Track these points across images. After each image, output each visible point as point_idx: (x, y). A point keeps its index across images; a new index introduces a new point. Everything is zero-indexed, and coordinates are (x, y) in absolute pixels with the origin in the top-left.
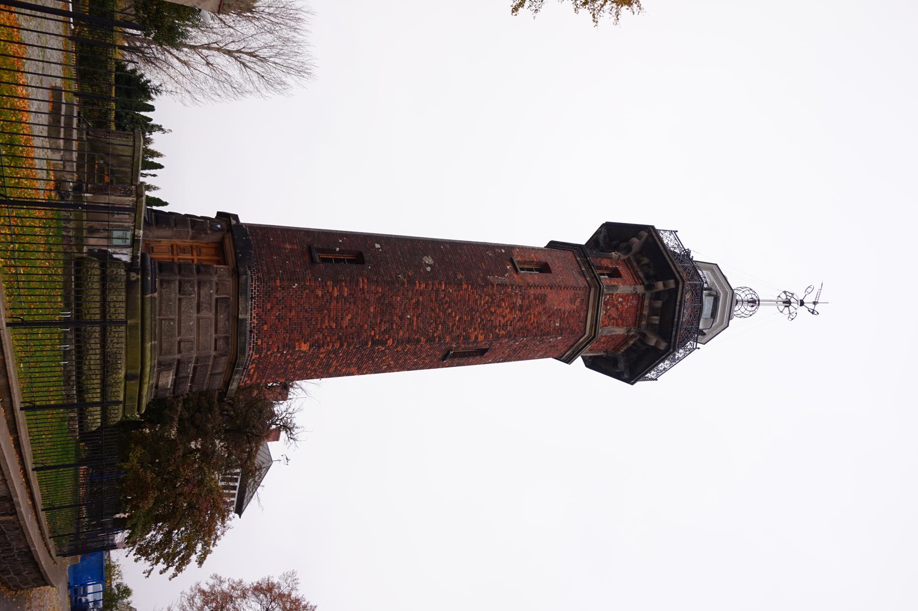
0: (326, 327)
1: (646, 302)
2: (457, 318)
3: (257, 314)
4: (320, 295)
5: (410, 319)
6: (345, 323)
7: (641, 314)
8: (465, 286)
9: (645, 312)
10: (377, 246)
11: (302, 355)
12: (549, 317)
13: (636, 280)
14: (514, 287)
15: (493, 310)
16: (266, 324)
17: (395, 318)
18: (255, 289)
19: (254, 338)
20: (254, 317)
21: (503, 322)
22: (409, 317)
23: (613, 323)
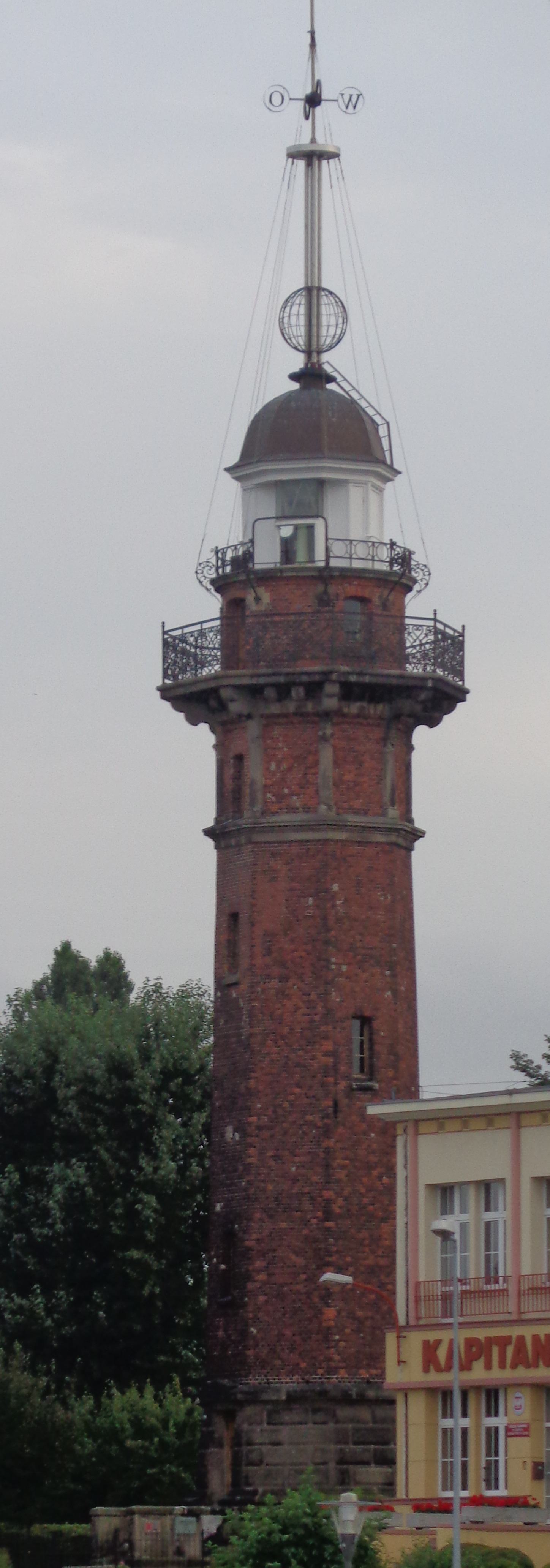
1: (275, 709)
2: (297, 1090)
5: (298, 1167)
11: (344, 1314)
14: (253, 996)
16: (298, 1364)
17: (295, 1191)
19: (315, 1378)
20: (291, 1379)
22: (294, 1169)
23: (314, 774)
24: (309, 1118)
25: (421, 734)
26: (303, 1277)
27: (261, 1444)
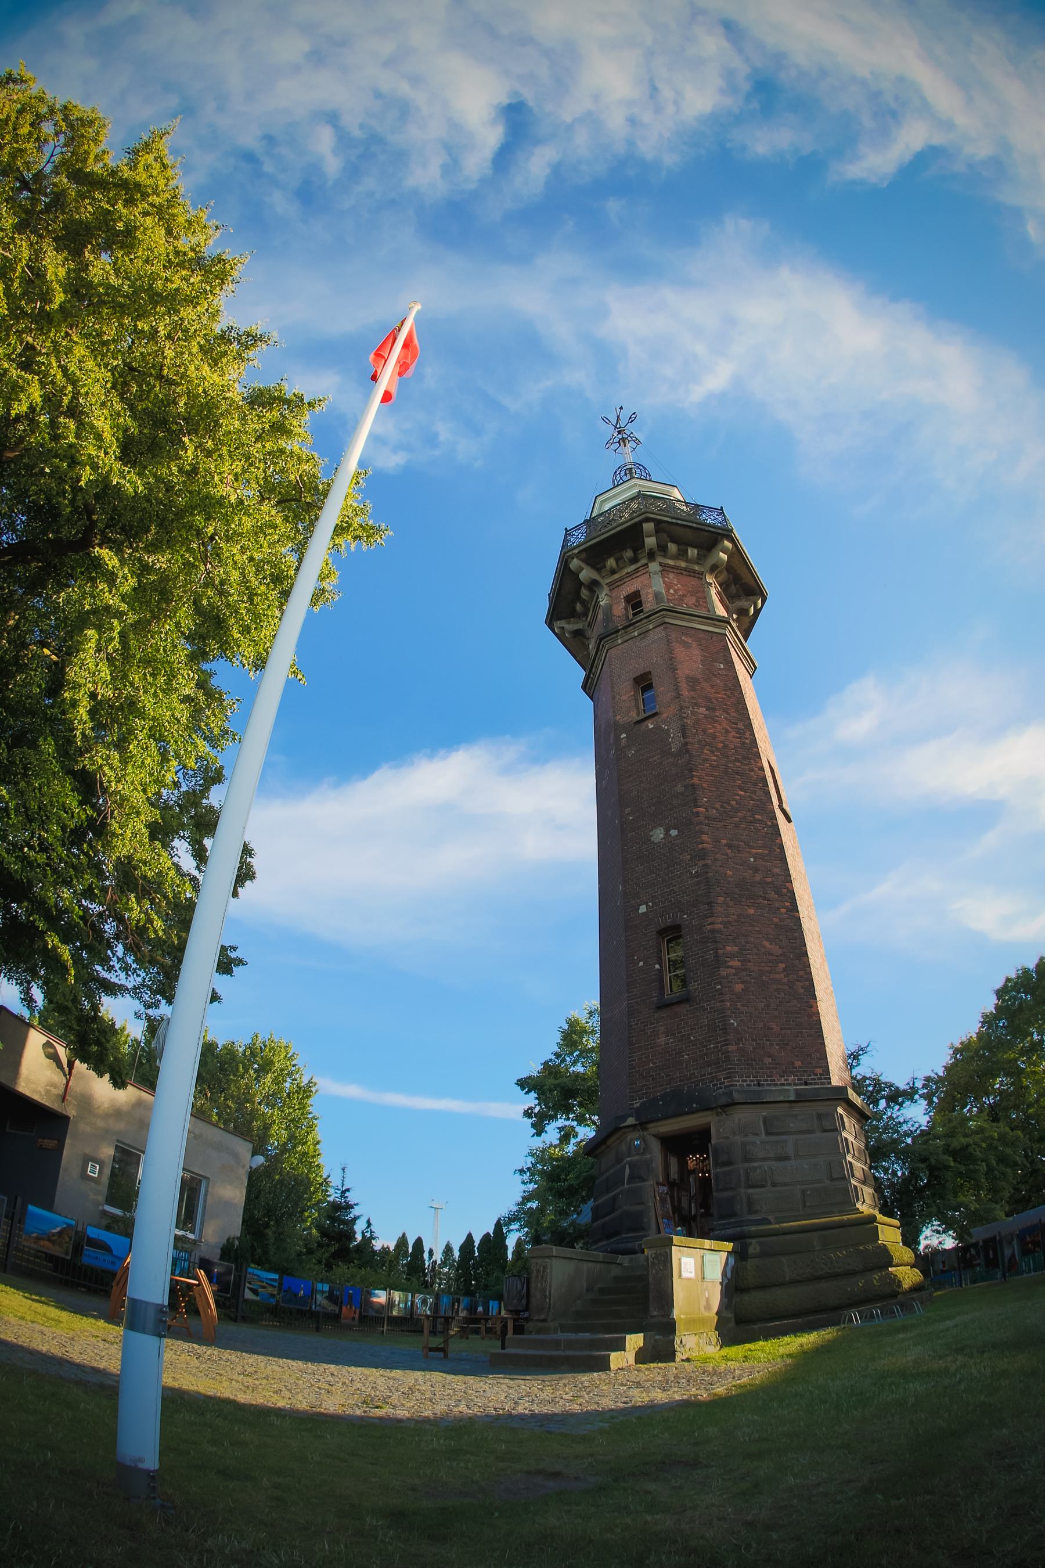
0: (785, 977)
1: (671, 562)
2: (741, 793)
3: (781, 1076)
4: (742, 986)
6: (776, 949)
7: (685, 569)
8: (695, 780)
9: (683, 564)
10: (643, 909)
12: (713, 674)
13: (640, 573)
14: (685, 715)
15: (720, 745)
16: (793, 1064)
17: (757, 878)
18: (746, 1081)
19: (814, 1079)
20: (785, 1080)
21: (733, 734)
22: (752, 860)
27: (764, 1159)
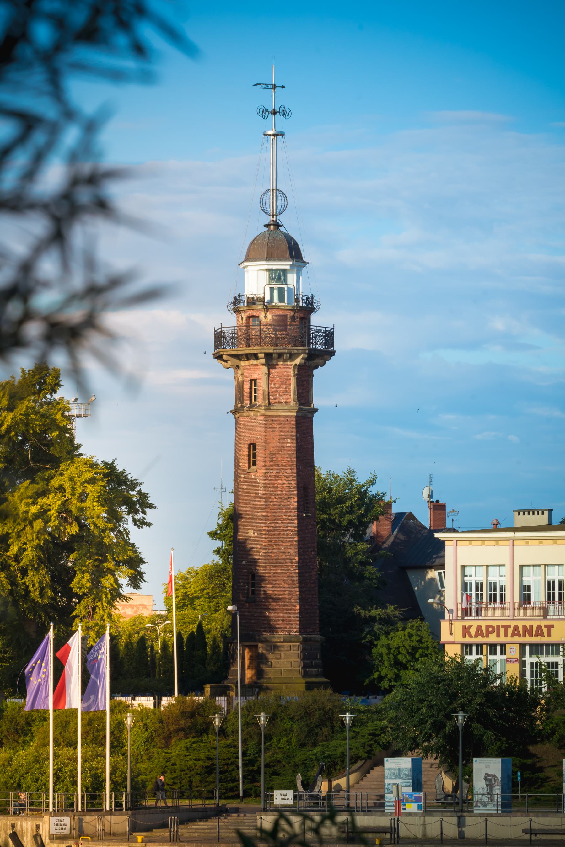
2: (284, 517)
6: (286, 585)
15: (279, 492)
17: (284, 557)
21: (287, 484)
24: (289, 528)
25: (314, 370)
26: (288, 592)
